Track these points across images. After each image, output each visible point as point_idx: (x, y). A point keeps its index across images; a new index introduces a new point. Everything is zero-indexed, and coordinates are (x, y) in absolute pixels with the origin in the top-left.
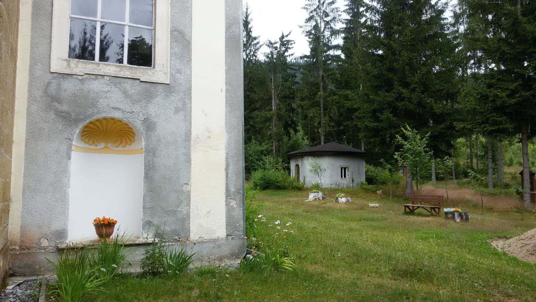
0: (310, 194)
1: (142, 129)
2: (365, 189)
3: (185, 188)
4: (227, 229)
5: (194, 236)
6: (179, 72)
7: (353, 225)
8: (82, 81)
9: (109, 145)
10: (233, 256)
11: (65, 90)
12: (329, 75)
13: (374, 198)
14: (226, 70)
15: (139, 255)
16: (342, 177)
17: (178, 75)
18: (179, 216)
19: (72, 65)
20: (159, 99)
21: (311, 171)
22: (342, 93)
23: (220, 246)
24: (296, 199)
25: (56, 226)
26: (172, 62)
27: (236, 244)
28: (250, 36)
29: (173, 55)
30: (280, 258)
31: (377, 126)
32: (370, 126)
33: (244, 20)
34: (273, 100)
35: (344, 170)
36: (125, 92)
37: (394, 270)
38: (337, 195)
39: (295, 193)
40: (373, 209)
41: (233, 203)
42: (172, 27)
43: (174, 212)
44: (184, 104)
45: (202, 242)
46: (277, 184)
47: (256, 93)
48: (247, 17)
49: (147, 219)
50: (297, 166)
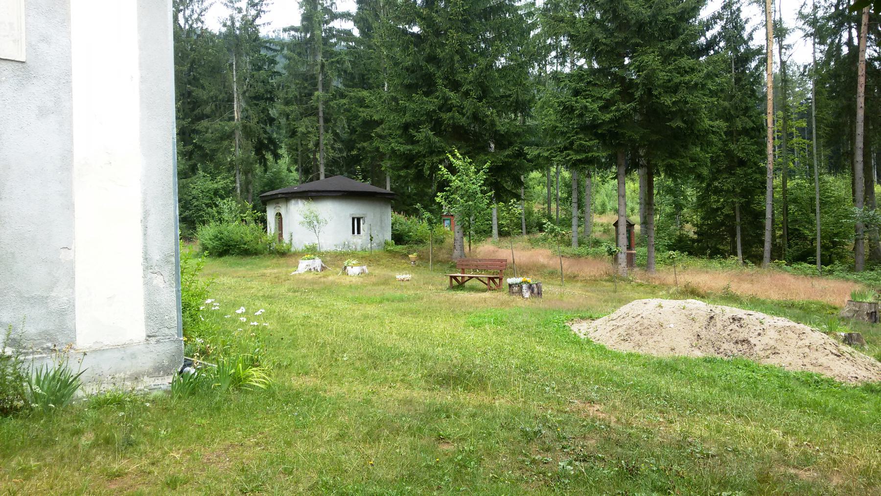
0: (301, 261)
2: (390, 252)
4: (147, 325)
5: (83, 341)
6: (45, 39)
7: (371, 309)
10: (159, 370)
12: (332, 62)
13: (404, 266)
21: (302, 223)
22: (355, 94)
23: (133, 356)
24: (275, 271)
30: (245, 368)
31: (410, 150)
32: (399, 150)
34: (235, 103)
35: (357, 223)
37: (429, 376)
38: (346, 263)
39: (275, 261)
40: (403, 284)
41: (158, 281)
46: (243, 246)
47: (203, 87)
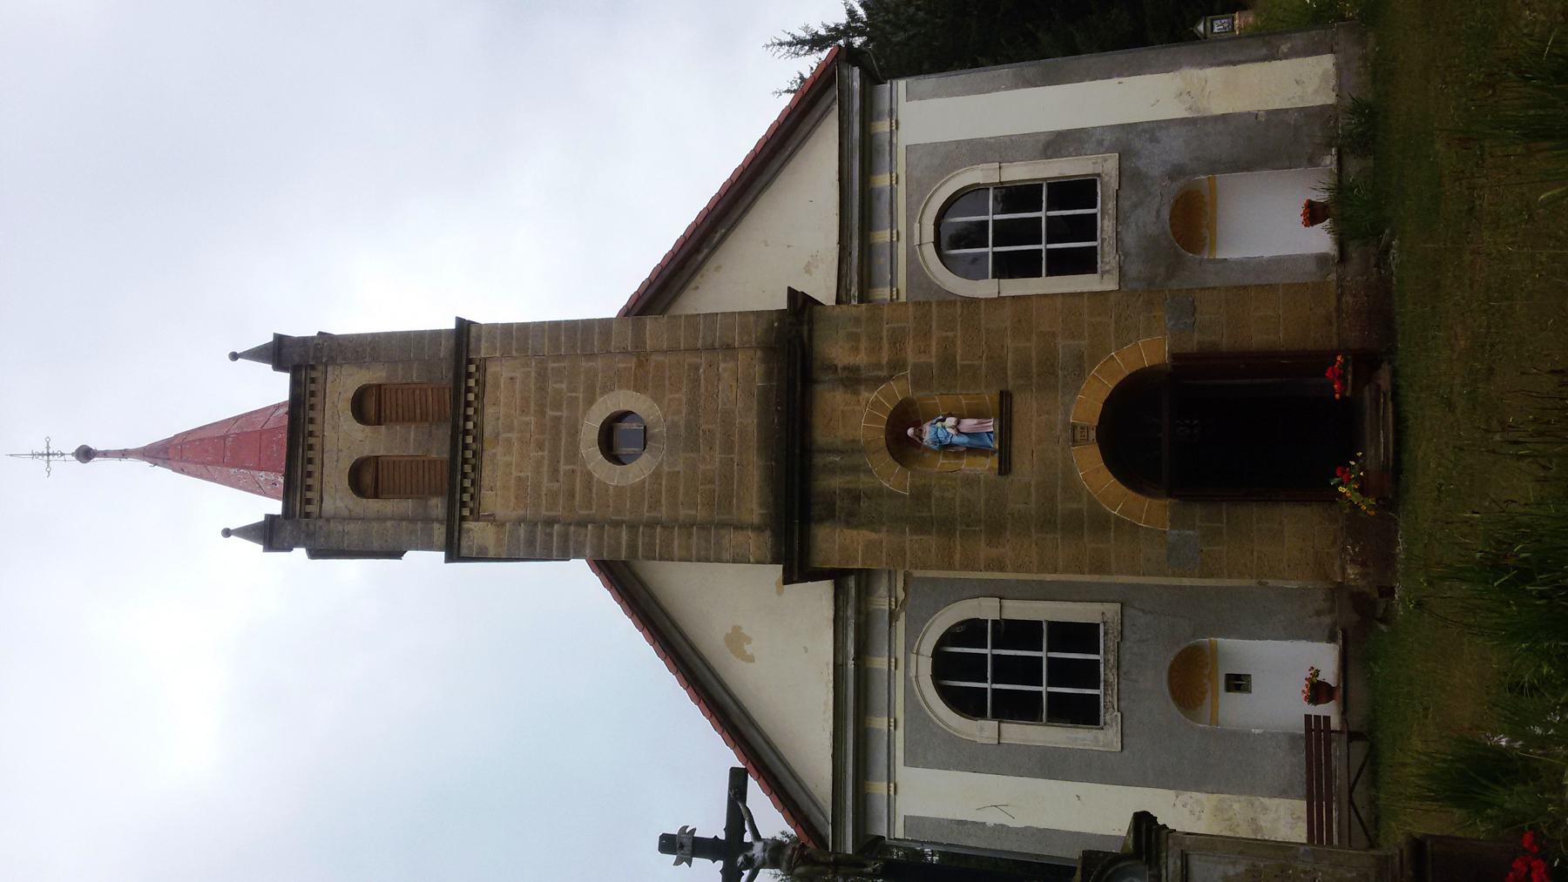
1: (1182, 181)
5: (1331, 99)
6: (1100, 143)
8: (1126, 255)
11: (1140, 272)
14: (1091, 80)
15: (1353, 165)
17: (1106, 143)
19: (1107, 268)
20: (1141, 164)
25: (1312, 267)
26: (1089, 152)
28: (848, 26)
33: (811, 49)
36: (1135, 206)
41: (1284, 48)
44: (1145, 131)
45: (1340, 88)
48: (802, 42)
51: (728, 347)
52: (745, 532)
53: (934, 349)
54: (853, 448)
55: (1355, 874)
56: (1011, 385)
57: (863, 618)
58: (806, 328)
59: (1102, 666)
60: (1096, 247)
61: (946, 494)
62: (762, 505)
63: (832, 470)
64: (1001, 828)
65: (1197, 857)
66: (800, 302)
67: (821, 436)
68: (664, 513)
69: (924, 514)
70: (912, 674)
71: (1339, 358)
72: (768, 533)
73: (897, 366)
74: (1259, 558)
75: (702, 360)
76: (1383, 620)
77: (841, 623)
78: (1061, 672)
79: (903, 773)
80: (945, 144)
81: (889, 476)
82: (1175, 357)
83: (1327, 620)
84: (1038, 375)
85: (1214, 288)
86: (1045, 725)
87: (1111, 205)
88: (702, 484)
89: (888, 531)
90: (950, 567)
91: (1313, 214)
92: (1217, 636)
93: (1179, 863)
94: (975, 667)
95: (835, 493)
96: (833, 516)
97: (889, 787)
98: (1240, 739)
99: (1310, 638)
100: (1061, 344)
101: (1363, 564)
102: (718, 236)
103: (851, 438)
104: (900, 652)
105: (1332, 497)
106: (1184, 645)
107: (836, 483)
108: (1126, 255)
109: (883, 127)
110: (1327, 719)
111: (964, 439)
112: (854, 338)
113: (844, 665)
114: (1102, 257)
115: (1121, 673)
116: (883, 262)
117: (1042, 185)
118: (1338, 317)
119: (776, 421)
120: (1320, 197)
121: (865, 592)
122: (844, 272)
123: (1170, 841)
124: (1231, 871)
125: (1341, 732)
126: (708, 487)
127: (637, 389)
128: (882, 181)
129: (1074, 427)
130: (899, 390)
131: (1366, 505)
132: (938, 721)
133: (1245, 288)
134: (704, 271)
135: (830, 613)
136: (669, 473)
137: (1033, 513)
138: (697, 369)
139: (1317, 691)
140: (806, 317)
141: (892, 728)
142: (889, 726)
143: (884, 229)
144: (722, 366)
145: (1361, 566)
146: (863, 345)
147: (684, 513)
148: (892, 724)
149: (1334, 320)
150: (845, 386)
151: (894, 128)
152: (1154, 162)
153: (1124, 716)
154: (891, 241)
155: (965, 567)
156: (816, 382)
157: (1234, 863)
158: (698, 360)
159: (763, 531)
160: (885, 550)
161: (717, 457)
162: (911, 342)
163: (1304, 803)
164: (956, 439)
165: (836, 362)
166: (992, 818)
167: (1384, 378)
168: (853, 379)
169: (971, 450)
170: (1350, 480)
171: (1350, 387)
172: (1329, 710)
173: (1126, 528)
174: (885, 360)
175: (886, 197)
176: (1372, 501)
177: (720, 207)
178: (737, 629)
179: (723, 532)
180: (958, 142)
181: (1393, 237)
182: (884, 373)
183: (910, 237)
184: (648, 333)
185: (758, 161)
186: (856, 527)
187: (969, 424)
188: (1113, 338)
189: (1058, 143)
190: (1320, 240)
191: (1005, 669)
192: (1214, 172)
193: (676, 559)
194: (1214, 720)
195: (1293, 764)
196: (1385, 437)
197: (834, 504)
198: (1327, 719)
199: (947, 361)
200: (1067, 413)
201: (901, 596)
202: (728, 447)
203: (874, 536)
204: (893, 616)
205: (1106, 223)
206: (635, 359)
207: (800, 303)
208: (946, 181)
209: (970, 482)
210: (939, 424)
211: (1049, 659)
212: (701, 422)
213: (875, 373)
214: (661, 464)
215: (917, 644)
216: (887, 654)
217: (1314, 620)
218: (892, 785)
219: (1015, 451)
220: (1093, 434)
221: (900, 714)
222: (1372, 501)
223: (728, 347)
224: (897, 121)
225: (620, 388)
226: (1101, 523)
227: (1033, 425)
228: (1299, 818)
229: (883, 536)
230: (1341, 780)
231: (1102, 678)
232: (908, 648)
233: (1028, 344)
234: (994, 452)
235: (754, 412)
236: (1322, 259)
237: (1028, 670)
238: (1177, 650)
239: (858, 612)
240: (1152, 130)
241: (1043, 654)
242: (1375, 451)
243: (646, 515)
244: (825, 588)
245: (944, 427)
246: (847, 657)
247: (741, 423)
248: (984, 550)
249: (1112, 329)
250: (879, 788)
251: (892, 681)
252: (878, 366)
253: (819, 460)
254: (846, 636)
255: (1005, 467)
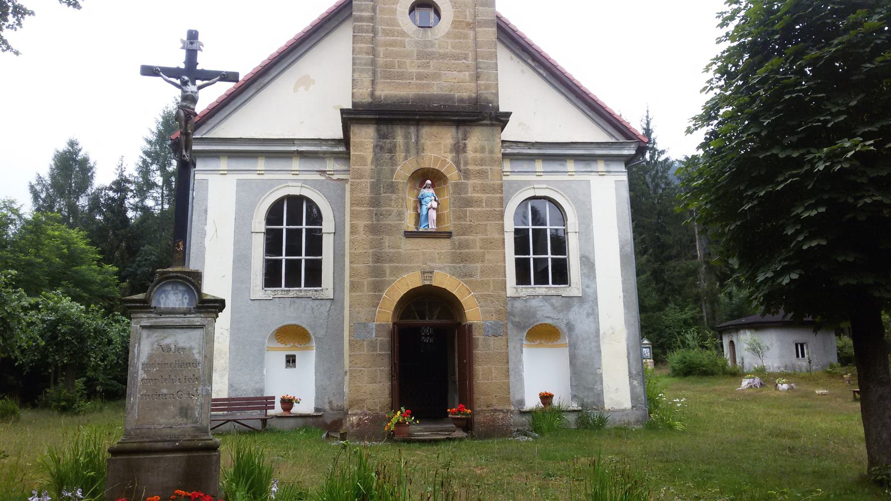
0: (743, 380)
1: (565, 330)
3: (598, 371)
4: (632, 402)
5: (607, 406)
6: (588, 286)
9: (543, 342)
10: (637, 422)
15: (572, 418)
16: (798, 356)
18: (596, 391)
19: (519, 291)
20: (575, 308)
21: (748, 350)
23: (627, 415)
24: (725, 387)
25: (518, 397)
27: (639, 413)
28: (655, 150)
29: (583, 275)
33: (644, 129)
34: (697, 243)
35: (800, 349)
36: (552, 305)
37: (770, 434)
38: (777, 381)
39: (726, 380)
41: (635, 383)
42: (581, 255)
43: (592, 389)
44: (593, 310)
46: (701, 368)
47: (669, 233)
48: (648, 124)
49: (574, 393)
50: (732, 343)
51: (478, 77)
52: (371, 86)
53: (476, 195)
54: (419, 149)
55: (197, 416)
56: (455, 238)
57: (321, 155)
58: (488, 122)
59: (298, 289)
60: (530, 284)
61: (393, 201)
62: (386, 96)
63: (407, 137)
64: (203, 234)
65: (202, 334)
66: (502, 119)
67: (426, 131)
68: (381, 38)
69: (382, 189)
70: (290, 184)
71: (469, 411)
72: (370, 100)
73: (466, 174)
74: (361, 370)
75: (470, 62)
76: (328, 435)
77: (318, 142)
78: (294, 266)
79: (233, 178)
80: (590, 202)
81: (404, 169)
82: (470, 326)
83: (327, 407)
84: (460, 253)
85: (508, 347)
86: (264, 258)
87: (553, 292)
88: (398, 61)
89: (372, 169)
90: (352, 204)
91: (546, 398)
92: (316, 350)
93: (198, 324)
94: (294, 218)
95: (394, 139)
96: (380, 138)
97: (225, 170)
98: (260, 362)
99: (317, 398)
100: (479, 265)
101: (358, 425)
102: (541, 71)
103: (425, 148)
104: (302, 177)
105: (394, 408)
106: (310, 332)
107: (400, 140)
108: (526, 300)
109: (601, 166)
110: (273, 408)
111: (424, 212)
112: (482, 150)
113: (294, 144)
114: (525, 288)
115: (294, 299)
116: (525, 166)
117: (565, 255)
118: (491, 410)
119: (435, 105)
120: (555, 402)
121: (336, 156)
122: (520, 145)
123: (210, 319)
124: (195, 351)
125: (266, 415)
126: (396, 64)
127: (454, 22)
128: (571, 166)
129: (432, 272)
130: (453, 175)
131: (391, 426)
132: (262, 199)
133: (508, 363)
134: (521, 63)
135: (322, 138)
136: (404, 41)
137: (383, 250)
138: (465, 58)
139: (288, 403)
140: (494, 122)
141: (258, 172)
142: (259, 171)
143: (543, 168)
144: (467, 73)
145: (357, 424)
146: (479, 155)
147: (381, 50)
148: (261, 172)
149: (490, 408)
150: (455, 145)
151: (600, 173)
152: (577, 315)
153: (271, 301)
154: (536, 172)
155: (352, 212)
156: (458, 128)
157: (199, 353)
158: (470, 59)
159: (371, 97)
160: (361, 167)
161: (415, 70)
162: (480, 182)
163: (227, 397)
164: (424, 208)
165: (469, 139)
166: (209, 228)
167: (459, 434)
168: (459, 149)
169: (418, 216)
170: (404, 417)
171: (454, 416)
172: (278, 409)
173: (376, 302)
174: (468, 167)
175: (561, 168)
176: (393, 428)
177: (558, 73)
178: (313, 82)
179: (370, 73)
180: (590, 210)
181: (535, 438)
182: (462, 167)
183: (539, 182)
184: (487, 29)
185: (584, 95)
186: (374, 151)
187: (433, 214)
188: (481, 293)
189: (588, 263)
190: (532, 402)
191: (294, 236)
192: (570, 346)
193: (354, 46)
194: (269, 349)
195: (247, 390)
196: (427, 435)
197: (388, 139)
198: (273, 408)
199: (469, 203)
200: (440, 269)
201: (335, 177)
202: (420, 77)
203: (369, 160)
204: (323, 172)
205: (544, 290)
206: (471, 21)
207: (501, 120)
208: (568, 202)
209: (400, 215)
210: (433, 198)
211: (301, 260)
212: (435, 61)
213: (462, 162)
214: (409, 36)
215: (307, 186)
216: (301, 169)
217: (327, 401)
218: (225, 172)
219: (417, 240)
220: (427, 283)
221: (267, 176)
222: (393, 428)
223: (478, 77)
224: (604, 175)
225: (455, 12)
226: (378, 287)
227: (432, 250)
228: (218, 394)
229: (369, 167)
230: (238, 415)
231: (291, 289)
232: (305, 181)
233: (478, 247)
234: (417, 228)
235: (440, 92)
236: (521, 402)
237: (294, 249)
238: (308, 329)
239: (325, 153)
240: (594, 314)
241: (303, 257)
242: (419, 430)
243: (380, 28)
244: (339, 135)
245: (431, 201)
246: (299, 146)
247: (434, 84)
248: (362, 223)
249: (486, 293)
250: (223, 164)
251: (285, 172)
252: (466, 163)
253: (412, 129)
254: (310, 145)
255: (409, 235)
